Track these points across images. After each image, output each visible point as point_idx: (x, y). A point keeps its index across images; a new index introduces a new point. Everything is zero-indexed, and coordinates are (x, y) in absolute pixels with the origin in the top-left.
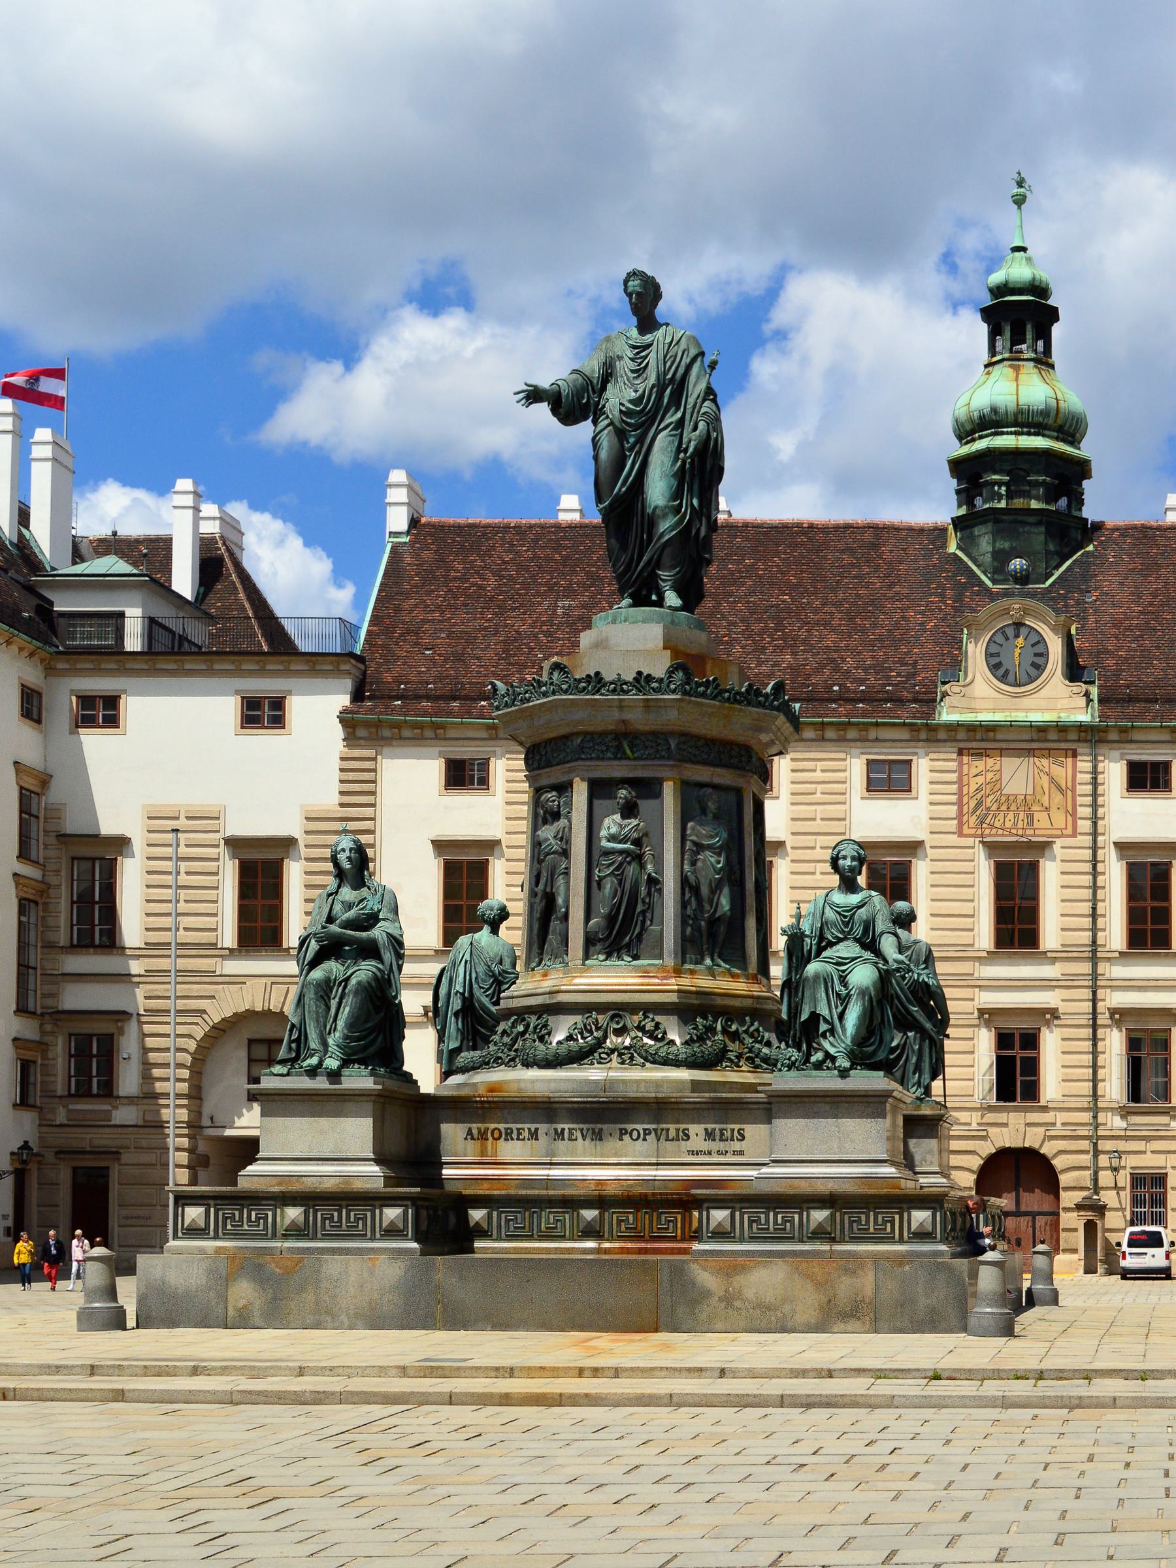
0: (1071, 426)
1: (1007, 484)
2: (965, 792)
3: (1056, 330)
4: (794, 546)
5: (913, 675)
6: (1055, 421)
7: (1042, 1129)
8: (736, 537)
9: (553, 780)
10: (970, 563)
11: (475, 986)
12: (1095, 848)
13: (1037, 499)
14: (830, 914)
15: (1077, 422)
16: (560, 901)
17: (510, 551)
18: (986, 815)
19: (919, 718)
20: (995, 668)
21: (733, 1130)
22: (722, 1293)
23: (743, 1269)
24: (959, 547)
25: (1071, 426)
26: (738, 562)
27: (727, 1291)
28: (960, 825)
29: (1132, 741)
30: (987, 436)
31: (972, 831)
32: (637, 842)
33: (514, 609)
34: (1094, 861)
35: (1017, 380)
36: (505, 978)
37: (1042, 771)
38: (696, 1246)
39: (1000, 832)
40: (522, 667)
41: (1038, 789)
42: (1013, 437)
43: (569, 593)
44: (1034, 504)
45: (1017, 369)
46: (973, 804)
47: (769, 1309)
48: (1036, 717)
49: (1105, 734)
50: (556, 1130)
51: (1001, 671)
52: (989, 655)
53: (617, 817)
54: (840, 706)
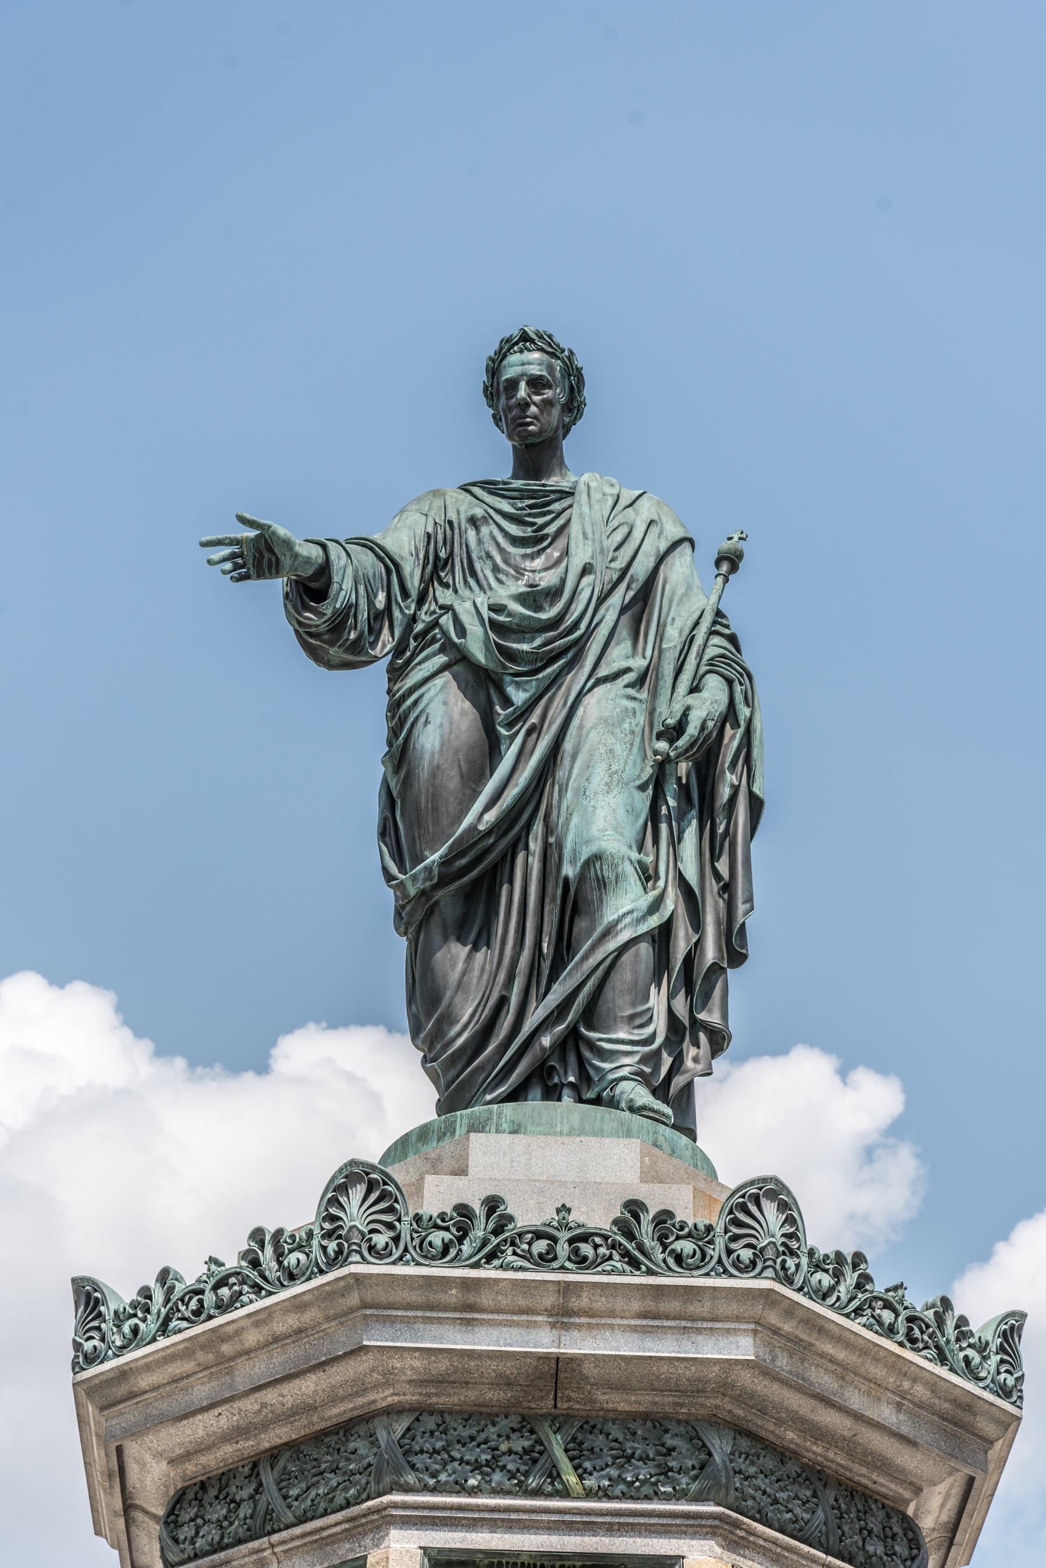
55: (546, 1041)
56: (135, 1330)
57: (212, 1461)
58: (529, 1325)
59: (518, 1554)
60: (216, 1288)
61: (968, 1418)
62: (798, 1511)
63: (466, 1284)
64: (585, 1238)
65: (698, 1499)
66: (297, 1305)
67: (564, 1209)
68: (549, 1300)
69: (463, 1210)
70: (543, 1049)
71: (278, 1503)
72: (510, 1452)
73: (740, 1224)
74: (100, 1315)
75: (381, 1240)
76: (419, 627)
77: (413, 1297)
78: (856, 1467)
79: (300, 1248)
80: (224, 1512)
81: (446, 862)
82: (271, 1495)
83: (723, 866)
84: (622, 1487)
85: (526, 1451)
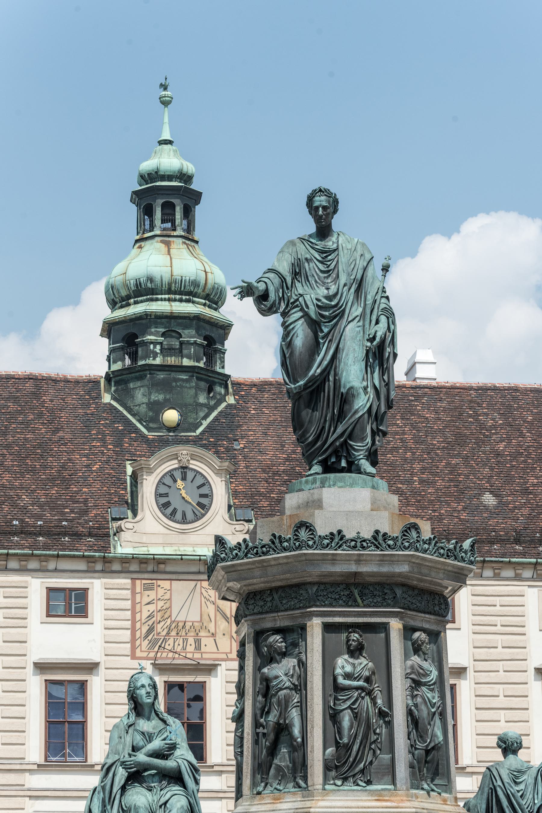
0: (216, 294)
1: (161, 343)
2: (138, 617)
3: (199, 211)
6: (203, 291)
9: (279, 624)
10: (125, 413)
13: (189, 357)
15: (221, 290)
16: (296, 731)
18: (157, 640)
19: (96, 551)
20: (164, 506)
24: (114, 398)
25: (216, 294)
28: (133, 649)
30: (142, 302)
31: (145, 655)
32: (368, 680)
35: (169, 253)
37: (208, 600)
39: (171, 655)
41: (205, 617)
42: (167, 303)
44: (186, 362)
45: (168, 244)
46: (145, 629)
49: (127, 565)
51: (169, 510)
53: (346, 657)
55: (338, 444)
56: (237, 554)
57: (257, 587)
58: (349, 564)
59: (347, 623)
60: (262, 547)
61: (461, 572)
62: (418, 604)
63: (333, 554)
64: (364, 541)
65: (393, 607)
66: (287, 557)
67: (358, 533)
68: (355, 558)
69: (332, 534)
70: (337, 446)
71: (280, 605)
72: (344, 595)
73: (404, 535)
74: (224, 547)
75: (311, 543)
76: (292, 300)
77: (320, 558)
78: (432, 586)
79: (287, 541)
80: (263, 603)
81: (305, 384)
82: (277, 601)
83: (386, 377)
84: (373, 604)
85: (348, 595)
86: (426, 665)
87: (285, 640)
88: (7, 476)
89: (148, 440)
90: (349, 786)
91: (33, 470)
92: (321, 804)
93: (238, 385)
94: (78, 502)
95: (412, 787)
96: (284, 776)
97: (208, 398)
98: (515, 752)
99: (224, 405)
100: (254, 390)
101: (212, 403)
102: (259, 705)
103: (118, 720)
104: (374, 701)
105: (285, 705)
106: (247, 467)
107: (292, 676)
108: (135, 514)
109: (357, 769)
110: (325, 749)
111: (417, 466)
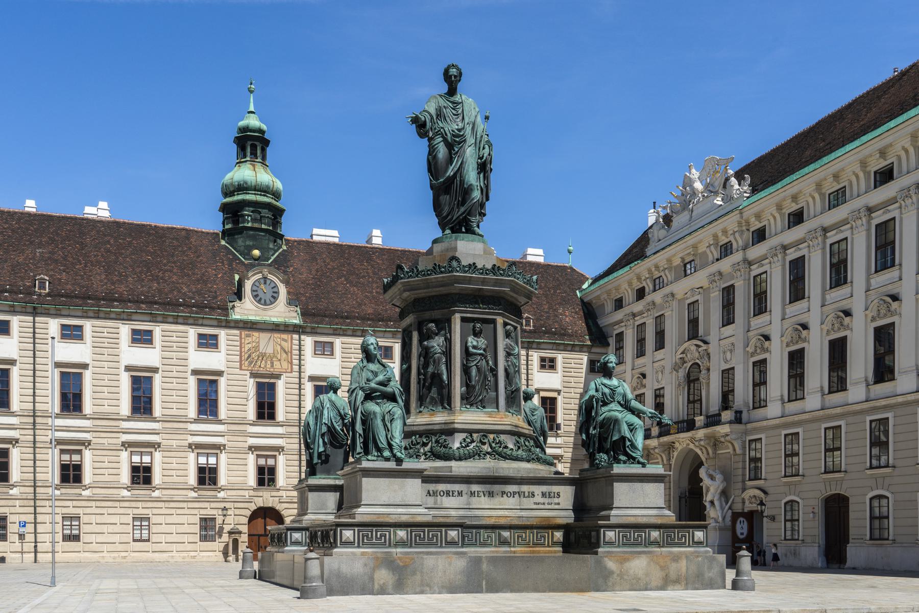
4: (150, 234)
5: (216, 297)
7: (278, 498)
8: (121, 228)
10: (233, 250)
11: (333, 421)
12: (300, 378)
14: (607, 391)
16: (445, 377)
17: (5, 223)
20: (255, 297)
21: (554, 493)
22: (618, 572)
23: (627, 560)
26: (124, 239)
27: (621, 571)
29: (316, 333)
33: (14, 251)
34: (300, 384)
36: (346, 417)
38: (600, 550)
40: (22, 279)
43: (40, 245)
47: (639, 579)
48: (274, 320)
50: (471, 492)
52: (253, 291)
53: (473, 337)
54: (185, 308)
86: (512, 344)
87: (437, 326)
88: (175, 277)
89: (245, 264)
90: (474, 409)
91: (188, 275)
92: (460, 418)
93: (288, 241)
94: (212, 292)
95: (506, 411)
96: (436, 403)
97: (274, 245)
98: (531, 399)
99: (281, 250)
100: (295, 243)
101: (276, 248)
102: (421, 363)
103: (356, 364)
104: (487, 362)
105: (437, 363)
106: (294, 280)
107: (442, 346)
108: (240, 299)
109: (478, 400)
110: (461, 388)
111: (375, 285)
